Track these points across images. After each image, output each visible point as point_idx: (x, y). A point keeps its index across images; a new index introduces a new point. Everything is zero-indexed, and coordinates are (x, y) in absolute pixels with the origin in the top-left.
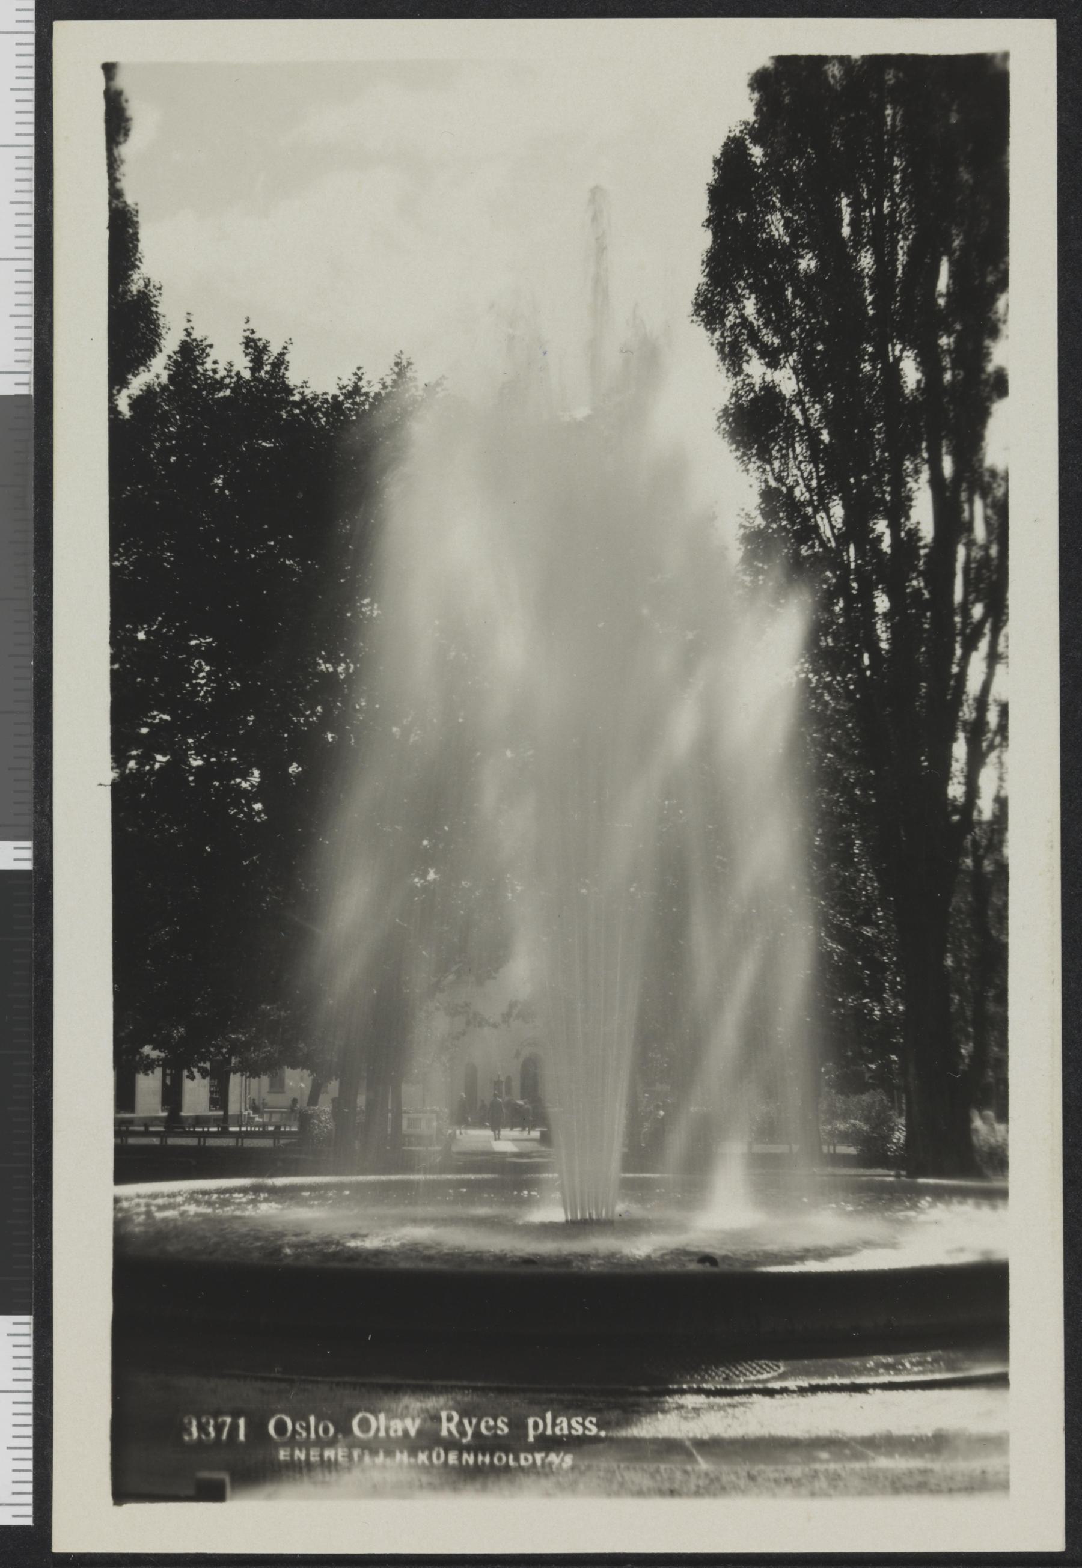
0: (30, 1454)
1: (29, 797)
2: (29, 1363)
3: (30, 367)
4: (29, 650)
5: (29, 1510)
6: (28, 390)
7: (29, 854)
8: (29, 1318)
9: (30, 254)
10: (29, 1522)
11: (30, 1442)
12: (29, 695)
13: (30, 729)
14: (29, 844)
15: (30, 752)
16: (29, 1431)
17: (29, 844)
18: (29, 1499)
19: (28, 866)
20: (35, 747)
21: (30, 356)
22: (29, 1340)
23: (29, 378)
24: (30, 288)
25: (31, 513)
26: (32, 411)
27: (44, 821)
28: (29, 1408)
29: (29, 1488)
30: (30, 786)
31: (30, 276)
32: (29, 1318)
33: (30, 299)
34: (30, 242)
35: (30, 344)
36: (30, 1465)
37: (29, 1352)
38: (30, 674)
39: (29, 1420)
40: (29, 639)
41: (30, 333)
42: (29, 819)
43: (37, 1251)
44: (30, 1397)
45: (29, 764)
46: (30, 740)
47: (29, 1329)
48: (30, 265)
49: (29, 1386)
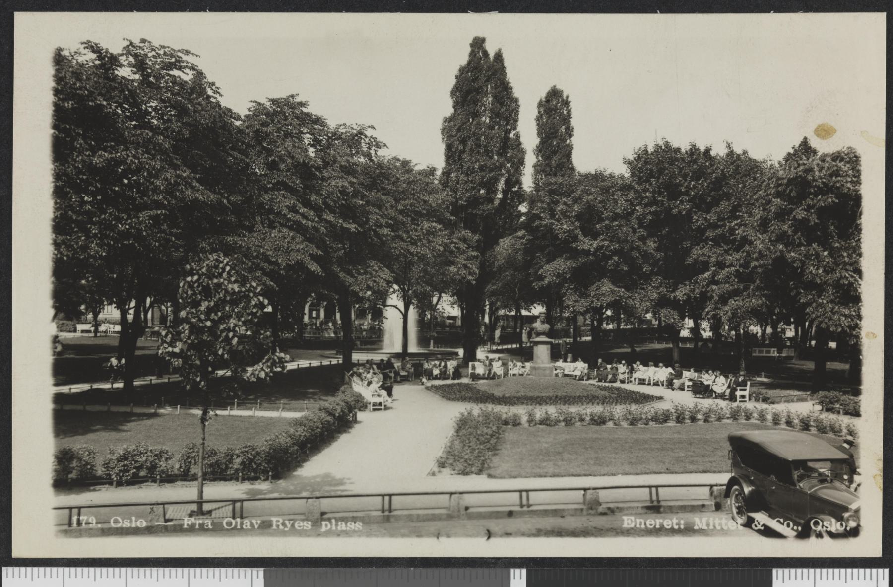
0: (849, 570)
1: (486, 570)
2: (799, 570)
3: (248, 570)
4: (405, 570)
5: (880, 570)
6: (261, 571)
7: (518, 571)
8: (774, 571)
9: (186, 570)
10: (887, 571)
11: (843, 570)
12: (430, 571)
13: (449, 570)
14: (512, 570)
15: (461, 570)
16: (837, 570)
17: (512, 570)
18: (874, 570)
19: (524, 571)
20: (459, 567)
21: (242, 570)
22: (787, 570)
23: (255, 570)
24: (205, 570)
25: (329, 569)
26: (273, 569)
27: (499, 562)
28: (824, 570)
29: (868, 570)
30: (480, 571)
31: (198, 570)
32: (774, 571)
33: (211, 570)
34: (179, 570)
35: (236, 570)
36: (855, 570)
37: (793, 570)
38: (418, 570)
39: (830, 570)
40: (398, 570)
41: (230, 570)
42: (498, 570)
43: (737, 566)
44: (818, 570)
45: (468, 570)
46: (455, 570)
47: (780, 571)
48: (192, 570)
49: (812, 570)
